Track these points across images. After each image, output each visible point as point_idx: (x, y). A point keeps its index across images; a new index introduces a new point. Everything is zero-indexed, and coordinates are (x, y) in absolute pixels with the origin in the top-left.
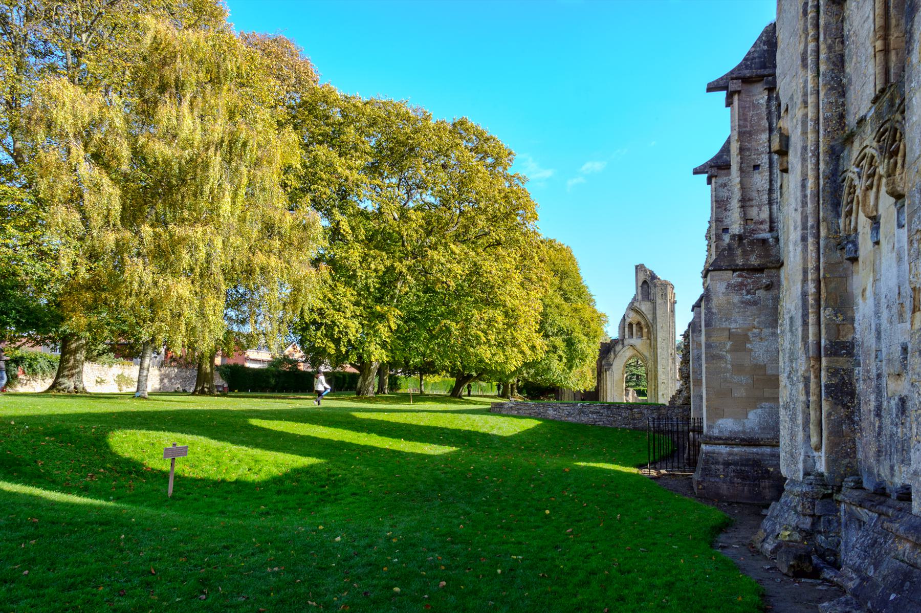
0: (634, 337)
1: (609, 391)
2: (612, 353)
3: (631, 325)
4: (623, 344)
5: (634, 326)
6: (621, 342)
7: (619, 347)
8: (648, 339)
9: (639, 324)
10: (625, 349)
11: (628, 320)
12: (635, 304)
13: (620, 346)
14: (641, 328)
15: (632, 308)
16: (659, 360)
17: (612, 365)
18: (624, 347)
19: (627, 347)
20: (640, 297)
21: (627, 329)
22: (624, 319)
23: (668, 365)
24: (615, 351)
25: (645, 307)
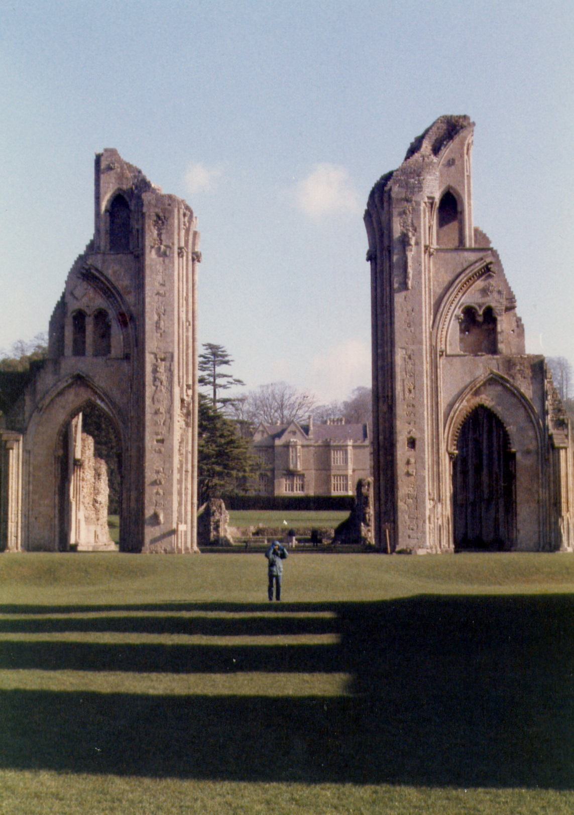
2: (27, 398)
7: (46, 380)
9: (101, 315)
11: (73, 306)
16: (148, 417)
22: (62, 306)
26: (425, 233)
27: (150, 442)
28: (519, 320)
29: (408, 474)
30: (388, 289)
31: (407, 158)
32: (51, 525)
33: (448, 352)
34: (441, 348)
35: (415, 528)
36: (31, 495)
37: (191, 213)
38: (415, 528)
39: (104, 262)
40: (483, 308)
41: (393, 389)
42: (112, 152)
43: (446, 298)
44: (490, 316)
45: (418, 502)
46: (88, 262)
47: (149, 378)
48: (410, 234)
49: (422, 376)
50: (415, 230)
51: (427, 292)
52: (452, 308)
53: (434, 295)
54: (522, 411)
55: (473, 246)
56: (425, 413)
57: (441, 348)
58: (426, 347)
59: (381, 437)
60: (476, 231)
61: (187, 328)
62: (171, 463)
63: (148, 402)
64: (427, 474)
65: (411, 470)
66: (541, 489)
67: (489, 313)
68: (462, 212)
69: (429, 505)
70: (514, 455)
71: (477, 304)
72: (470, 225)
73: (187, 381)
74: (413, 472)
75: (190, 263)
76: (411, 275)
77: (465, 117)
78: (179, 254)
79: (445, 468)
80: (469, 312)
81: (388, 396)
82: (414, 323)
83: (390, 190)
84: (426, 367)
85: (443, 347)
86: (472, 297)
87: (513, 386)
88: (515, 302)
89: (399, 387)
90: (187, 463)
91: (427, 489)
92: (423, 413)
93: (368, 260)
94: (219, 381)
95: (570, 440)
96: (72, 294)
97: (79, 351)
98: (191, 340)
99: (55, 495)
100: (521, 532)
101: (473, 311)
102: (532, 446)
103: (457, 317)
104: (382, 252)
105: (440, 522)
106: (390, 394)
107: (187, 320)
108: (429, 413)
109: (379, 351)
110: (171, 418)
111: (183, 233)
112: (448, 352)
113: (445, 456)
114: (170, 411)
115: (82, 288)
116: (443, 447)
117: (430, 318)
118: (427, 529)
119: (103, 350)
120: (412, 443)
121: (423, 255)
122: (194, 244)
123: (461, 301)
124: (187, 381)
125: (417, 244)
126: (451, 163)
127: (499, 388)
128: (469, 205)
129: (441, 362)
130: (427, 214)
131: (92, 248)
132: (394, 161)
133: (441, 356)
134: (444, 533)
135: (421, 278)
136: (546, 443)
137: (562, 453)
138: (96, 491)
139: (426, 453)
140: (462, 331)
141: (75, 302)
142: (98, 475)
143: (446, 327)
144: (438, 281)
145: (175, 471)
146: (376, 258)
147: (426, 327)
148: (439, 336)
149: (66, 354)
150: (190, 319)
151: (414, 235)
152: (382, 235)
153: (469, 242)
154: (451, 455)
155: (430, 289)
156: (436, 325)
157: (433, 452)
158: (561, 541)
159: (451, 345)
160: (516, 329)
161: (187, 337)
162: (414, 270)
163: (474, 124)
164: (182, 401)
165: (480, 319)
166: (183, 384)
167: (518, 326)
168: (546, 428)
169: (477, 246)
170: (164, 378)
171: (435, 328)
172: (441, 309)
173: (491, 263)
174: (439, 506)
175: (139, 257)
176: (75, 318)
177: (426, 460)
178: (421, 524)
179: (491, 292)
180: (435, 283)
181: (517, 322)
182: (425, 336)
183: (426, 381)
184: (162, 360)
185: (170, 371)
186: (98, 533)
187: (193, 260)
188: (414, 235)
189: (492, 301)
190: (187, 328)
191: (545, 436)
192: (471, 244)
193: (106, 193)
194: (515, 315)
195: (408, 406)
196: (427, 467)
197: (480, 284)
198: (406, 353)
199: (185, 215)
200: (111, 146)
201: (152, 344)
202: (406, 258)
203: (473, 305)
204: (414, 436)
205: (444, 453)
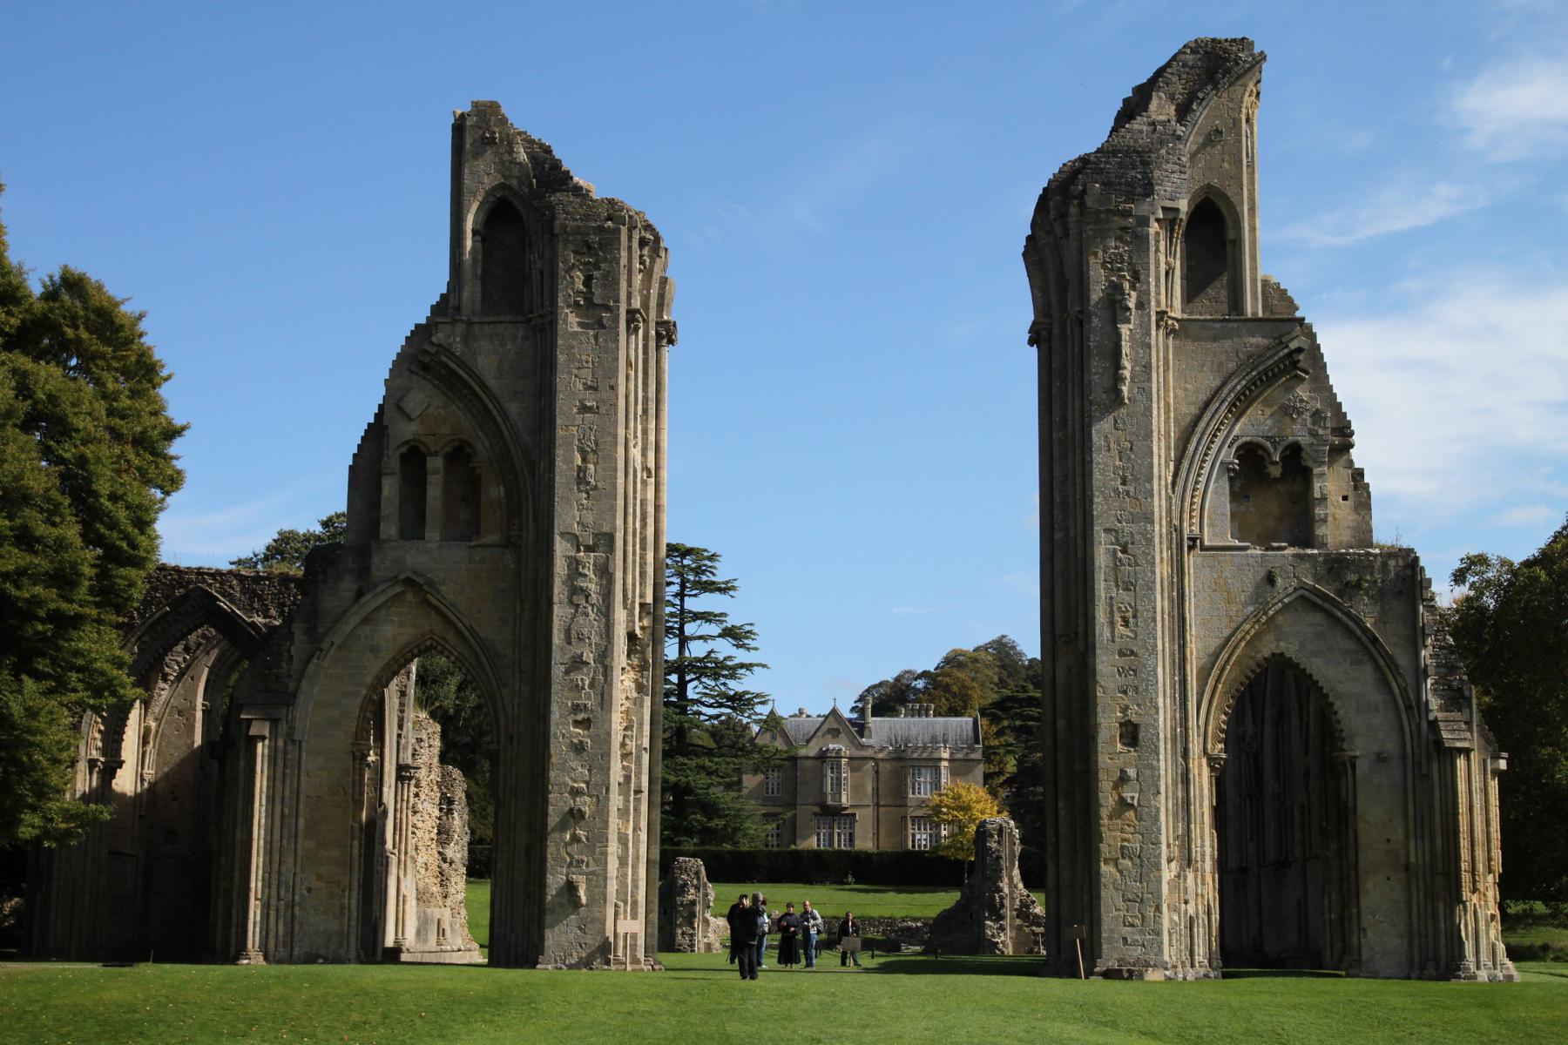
0: (433, 533)
3: (414, 458)
4: (363, 572)
5: (435, 463)
8: (509, 543)
9: (459, 455)
10: (370, 602)
11: (406, 431)
12: (439, 337)
13: (348, 586)
14: (474, 482)
16: (557, 671)
20: (471, 293)
21: (390, 488)
22: (376, 434)
23: (605, 700)
26: (1158, 286)
27: (563, 729)
28: (1358, 475)
29: (1123, 805)
30: (1077, 402)
31: (1114, 130)
32: (342, 907)
33: (1207, 543)
34: (1191, 531)
35: (1138, 922)
36: (300, 840)
37: (657, 239)
38: (1138, 922)
39: (466, 340)
40: (1280, 449)
41: (1089, 619)
42: (493, 107)
43: (1202, 425)
44: (1297, 466)
45: (1147, 865)
46: (434, 340)
47: (559, 591)
48: (1127, 285)
49: (1152, 589)
50: (1136, 277)
51: (1162, 411)
52: (1215, 447)
53: (1176, 418)
55: (1260, 314)
56: (1160, 670)
57: (1191, 531)
58: (1160, 529)
59: (1061, 723)
60: (1265, 283)
61: (644, 483)
62: (606, 770)
63: (557, 639)
64: (1164, 805)
65: (1130, 794)
66: (1412, 842)
68: (1237, 243)
69: (1168, 873)
70: (1353, 762)
71: (1268, 438)
72: (1254, 269)
73: (642, 596)
74: (1133, 798)
75: (652, 344)
76: (1127, 373)
77: (1244, 43)
78: (628, 323)
79: (1201, 790)
80: (1250, 454)
81: (1076, 634)
82: (1136, 477)
83: (1084, 192)
84: (1162, 570)
85: (1196, 529)
86: (1253, 424)
87: (1348, 614)
88: (1352, 434)
89: (1101, 616)
90: (638, 773)
91: (1163, 839)
92: (1155, 670)
93: (1031, 343)
94: (690, 629)
95: (1475, 734)
96: (399, 408)
98: (651, 509)
99: (353, 839)
100: (1370, 934)
101: (1260, 452)
102: (1391, 747)
103: (1226, 467)
104: (1063, 327)
105: (1191, 911)
106: (1081, 630)
107: (646, 468)
108: (1168, 671)
109: (1058, 536)
110: (607, 671)
111: (638, 279)
112: (1207, 543)
113: (1200, 766)
114: (604, 656)
115: (421, 398)
116: (1195, 747)
117: (1167, 466)
118: (1166, 925)
119: (465, 528)
120: (1131, 734)
121: (1153, 333)
122: (661, 306)
123: (1234, 433)
124: (642, 596)
125: (1141, 305)
126: (1212, 138)
127: (1319, 618)
128: (1253, 229)
129: (1191, 560)
130: (1162, 244)
131: (442, 309)
132: (1091, 135)
133: (1191, 548)
134: (1200, 932)
135: (1149, 380)
136: (1424, 739)
137: (1461, 763)
138: (444, 834)
139: (1162, 757)
140: (1234, 497)
142: (447, 803)
143: (1201, 486)
144: (1186, 389)
145: (614, 788)
146: (1049, 339)
147: (1160, 484)
148: (1187, 505)
149: (383, 536)
150: (651, 465)
151: (1133, 287)
152: (1063, 292)
153: (1253, 306)
154: (1211, 760)
155: (1167, 405)
156: (1180, 482)
157: (1174, 753)
158: (1462, 956)
159: (1211, 525)
160: (1351, 494)
161: (644, 503)
162: (1135, 361)
163: (1263, 57)
164: (631, 637)
165: (1275, 472)
166: (633, 602)
167: (1356, 488)
168: (1422, 707)
169: (1268, 315)
170: (593, 587)
171: (1179, 489)
172: (1191, 448)
174: (1190, 876)
175: (544, 332)
176: (403, 457)
177: (1162, 772)
178: (1150, 913)
179: (1300, 414)
180: (1181, 393)
181: (1354, 479)
182: (1159, 505)
183: (1161, 603)
184: (589, 549)
185: (605, 572)
186: (446, 926)
187: (659, 336)
188: (1133, 287)
189: (1299, 432)
190: (644, 483)
191: (1419, 725)
192: (1255, 313)
193: (474, 194)
194: (1351, 462)
195: (1121, 654)
196: (1163, 789)
198: (1117, 540)
199: (643, 243)
200: (485, 97)
201: (570, 514)
202: (1119, 336)
203: (1255, 439)
204: (1134, 719)
205: (1200, 758)
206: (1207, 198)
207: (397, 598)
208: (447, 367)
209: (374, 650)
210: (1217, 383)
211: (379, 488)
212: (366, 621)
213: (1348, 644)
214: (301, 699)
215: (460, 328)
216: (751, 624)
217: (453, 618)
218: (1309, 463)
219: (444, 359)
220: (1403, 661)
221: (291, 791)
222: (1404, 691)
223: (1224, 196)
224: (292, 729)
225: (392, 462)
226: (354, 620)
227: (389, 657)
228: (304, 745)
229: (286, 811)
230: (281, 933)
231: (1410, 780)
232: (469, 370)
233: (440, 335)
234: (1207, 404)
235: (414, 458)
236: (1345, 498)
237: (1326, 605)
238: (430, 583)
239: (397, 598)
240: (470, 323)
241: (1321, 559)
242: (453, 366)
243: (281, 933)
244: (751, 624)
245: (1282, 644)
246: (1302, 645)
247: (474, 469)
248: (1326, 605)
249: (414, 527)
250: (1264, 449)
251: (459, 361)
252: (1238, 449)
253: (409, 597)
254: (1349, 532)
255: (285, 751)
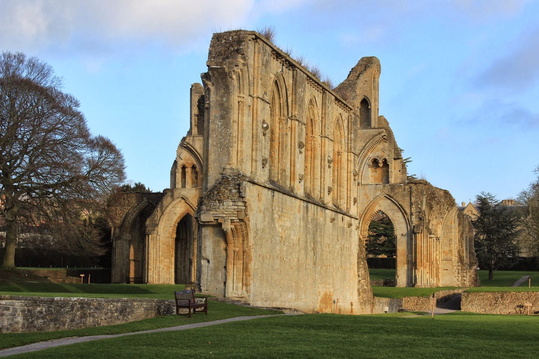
1: (151, 262)
2: (159, 209)
3: (184, 168)
4: (172, 196)
5: (189, 170)
6: (169, 194)
7: (167, 200)
10: (174, 203)
11: (180, 163)
12: (187, 140)
15: (184, 145)
17: (157, 225)
18: (173, 200)
19: (177, 201)
21: (179, 175)
22: (175, 162)
24: (162, 206)
25: (198, 146)
36: (160, 258)
39: (193, 140)
46: (186, 141)
54: (400, 213)
55: (377, 127)
67: (385, 162)
80: (375, 162)
97: (184, 186)
112: (362, 184)
115: (185, 154)
127: (389, 201)
131: (190, 133)
141: (181, 160)
149: (177, 187)
167: (403, 168)
173: (385, 136)
197: (380, 146)
203: (376, 158)
206: (364, 98)
207: (180, 201)
208: (189, 147)
209: (175, 214)
210: (364, 145)
211: (175, 176)
212: (173, 207)
213: (396, 208)
214: (159, 225)
215: (191, 138)
216: (415, 175)
217: (192, 206)
218: (389, 163)
219: (188, 145)
220: (408, 211)
221: (158, 246)
222: (408, 219)
223: (367, 97)
224: (158, 232)
225: (179, 170)
226: (170, 207)
227: (178, 215)
228: (161, 236)
229: (157, 251)
230: (157, 278)
231: (409, 240)
232: (194, 148)
233: (187, 140)
234: (362, 150)
235: (184, 168)
236: (400, 171)
237: (391, 198)
238: (187, 198)
239: (180, 201)
240: (193, 137)
241: (389, 187)
242: (190, 147)
243: (157, 278)
244: (415, 175)
245: (381, 208)
246: (385, 208)
247: (196, 171)
248: (391, 198)
249: (184, 186)
250: (378, 160)
251: (191, 146)
252: (372, 160)
253: (183, 201)
254: (400, 180)
255: (156, 237)
